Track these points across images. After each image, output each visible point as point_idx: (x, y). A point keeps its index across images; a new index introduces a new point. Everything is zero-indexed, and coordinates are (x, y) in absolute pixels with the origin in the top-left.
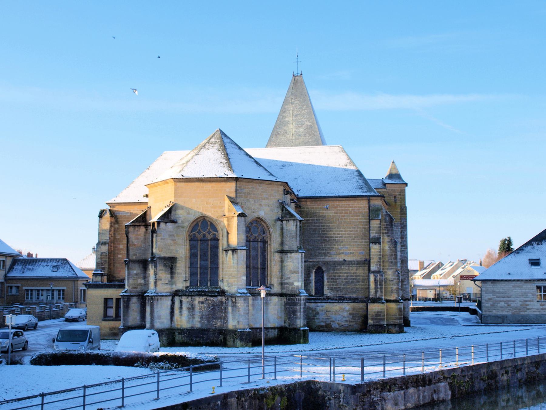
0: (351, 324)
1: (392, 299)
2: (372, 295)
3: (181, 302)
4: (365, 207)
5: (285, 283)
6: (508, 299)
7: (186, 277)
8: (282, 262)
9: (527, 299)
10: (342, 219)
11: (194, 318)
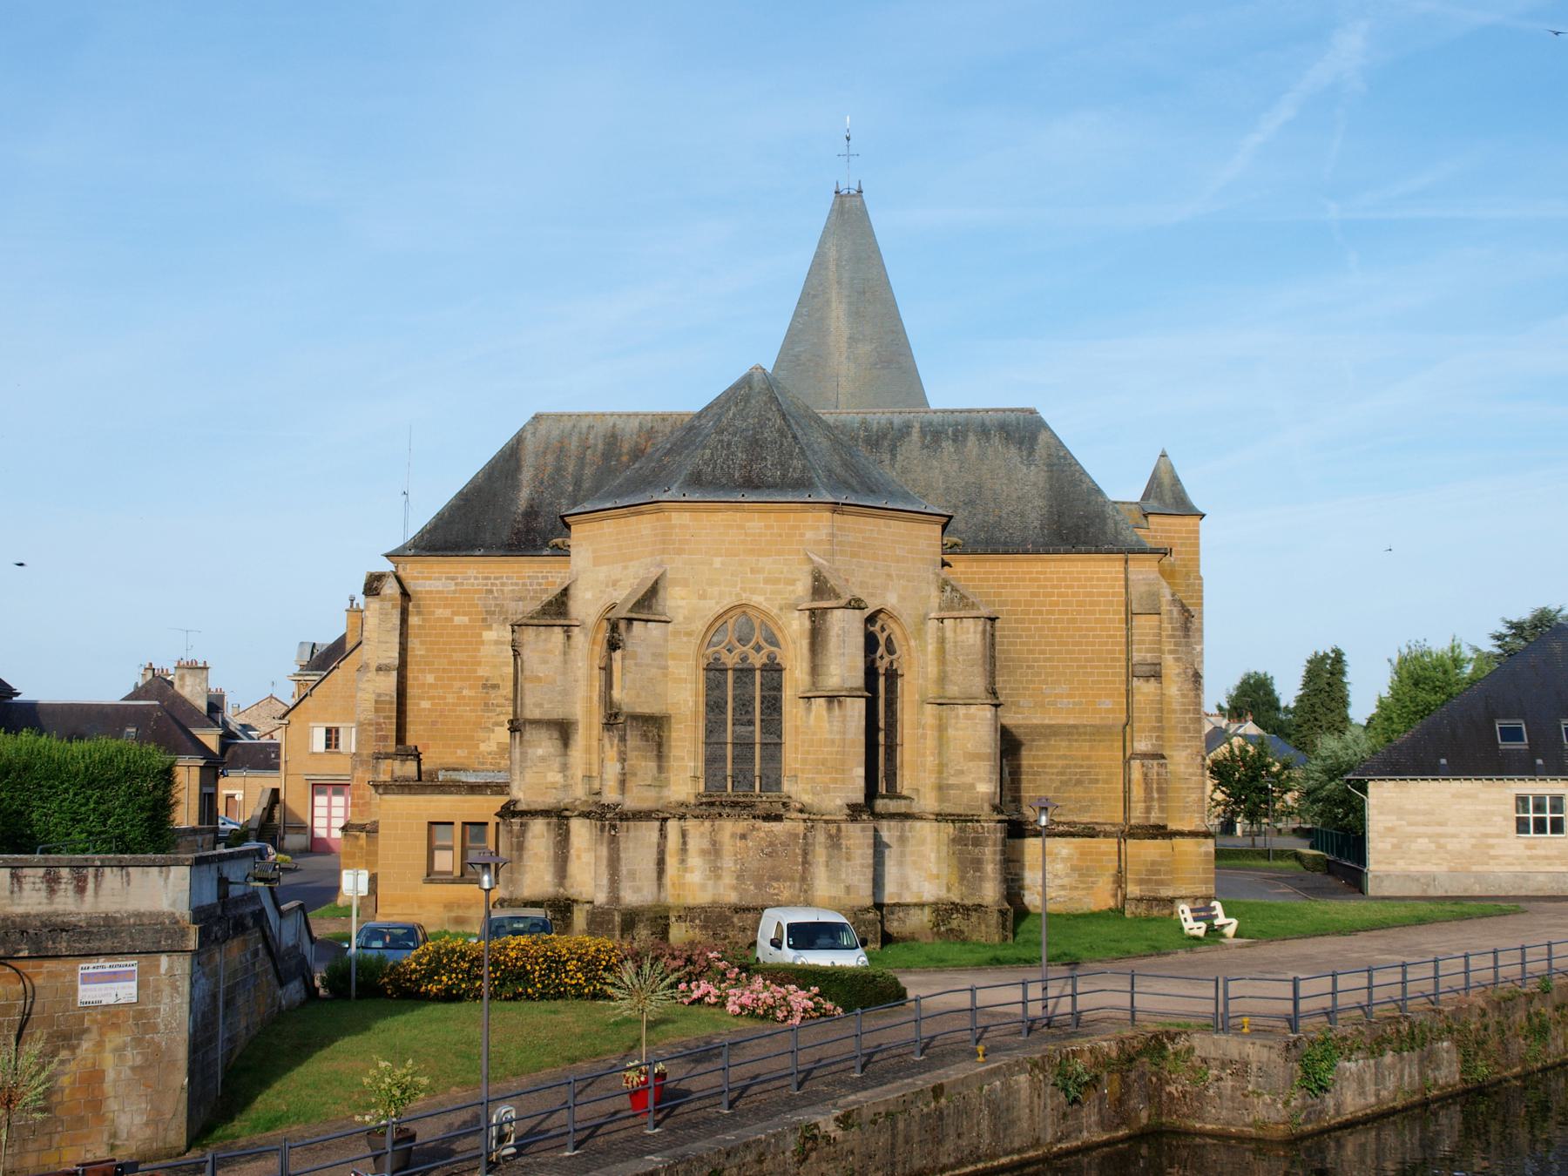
0: (1075, 894)
1: (1186, 829)
2: (1139, 817)
3: (684, 834)
4: (1115, 579)
5: (949, 787)
6: (1439, 830)
7: (696, 768)
8: (941, 728)
10: (1051, 612)
11: (718, 877)
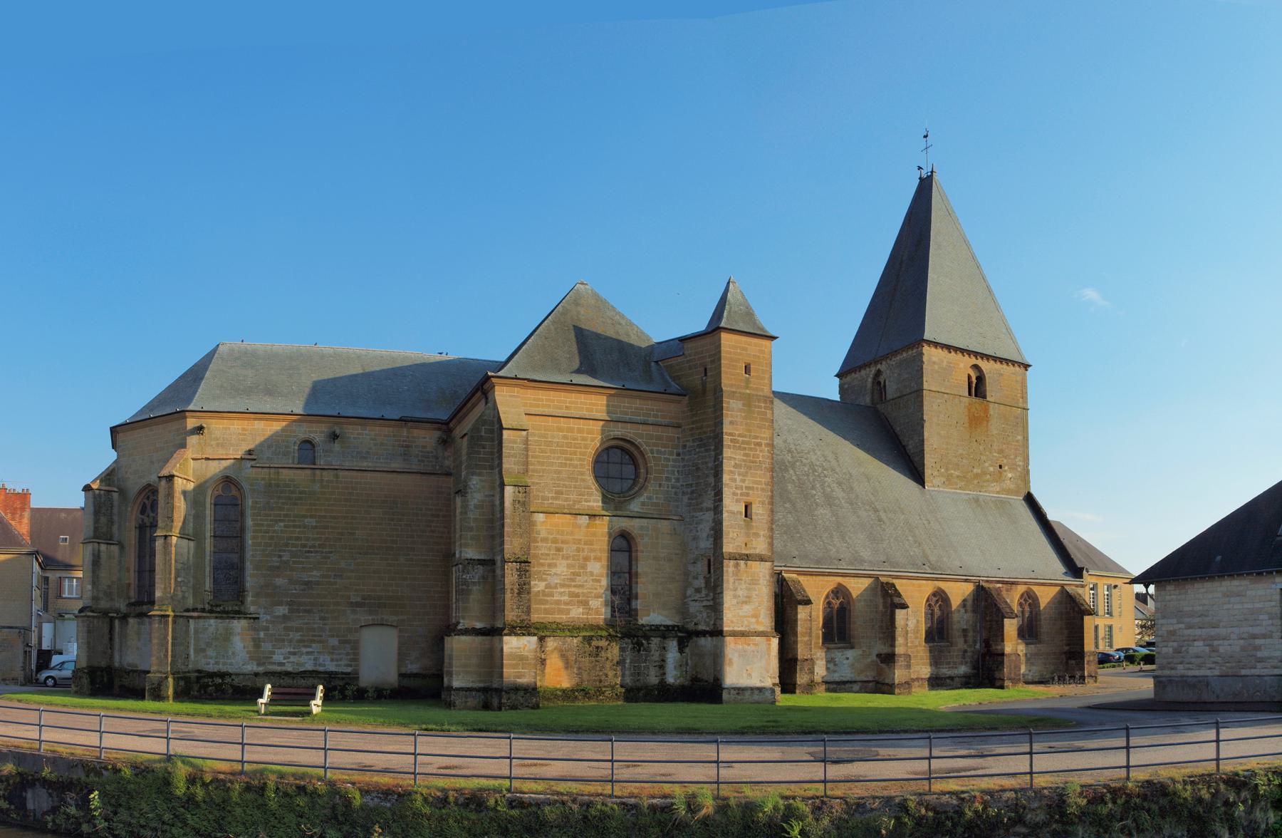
6: (1214, 632)
9: (1257, 630)
